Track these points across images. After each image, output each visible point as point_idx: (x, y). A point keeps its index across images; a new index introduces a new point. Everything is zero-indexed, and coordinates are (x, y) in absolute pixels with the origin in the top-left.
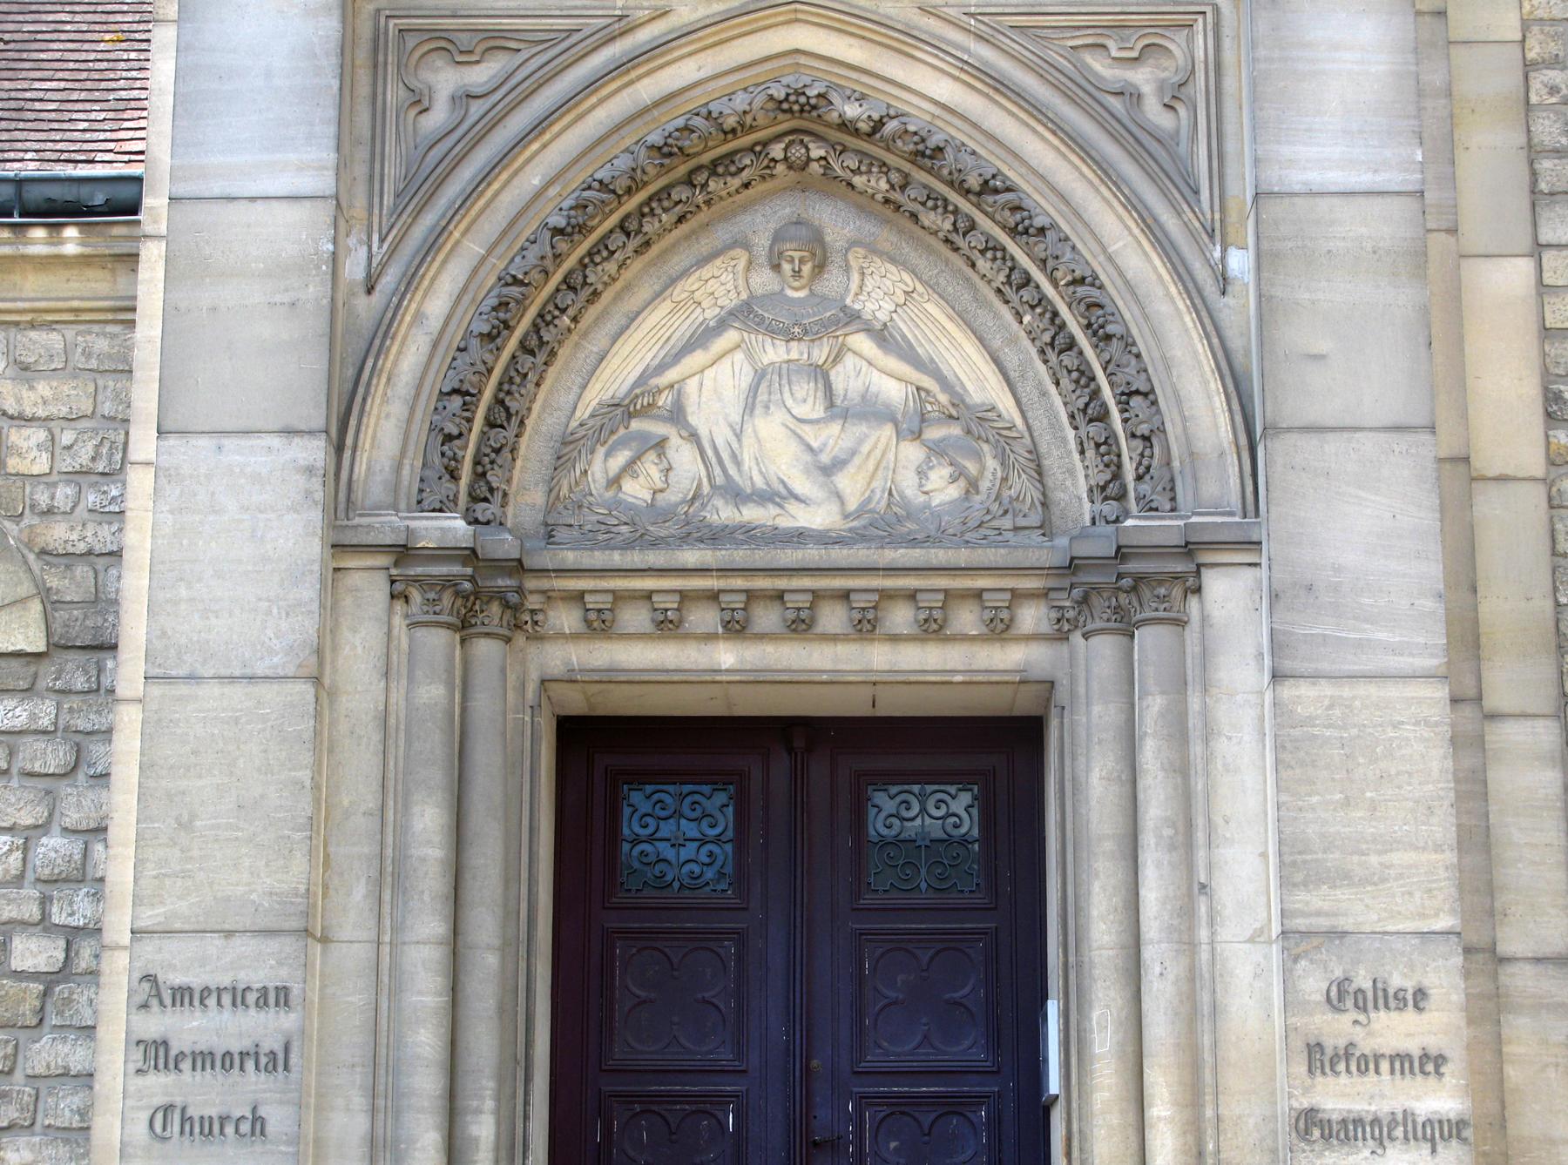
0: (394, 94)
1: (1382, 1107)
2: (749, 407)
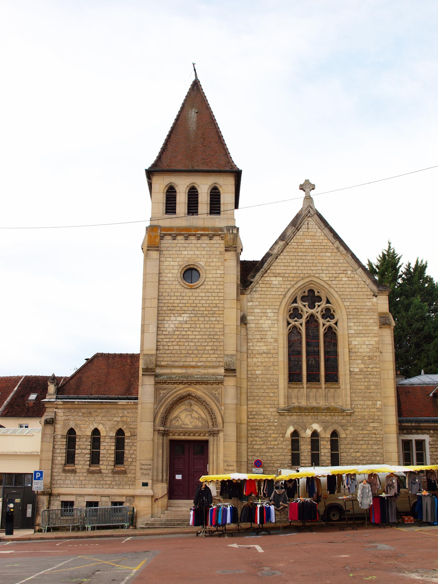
0: (158, 393)
2: (185, 417)
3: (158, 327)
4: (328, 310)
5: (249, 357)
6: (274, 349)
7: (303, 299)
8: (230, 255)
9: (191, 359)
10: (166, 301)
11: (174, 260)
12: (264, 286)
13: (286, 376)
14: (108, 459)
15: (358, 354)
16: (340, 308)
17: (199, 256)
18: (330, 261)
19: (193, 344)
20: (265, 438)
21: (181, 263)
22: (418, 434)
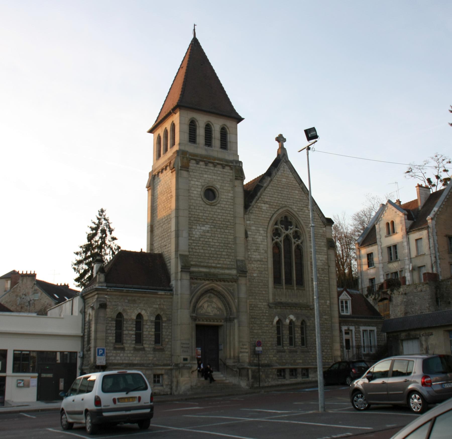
6: (265, 258)
8: (237, 183)
12: (257, 209)
14: (150, 339)
19: (213, 249)
21: (203, 184)
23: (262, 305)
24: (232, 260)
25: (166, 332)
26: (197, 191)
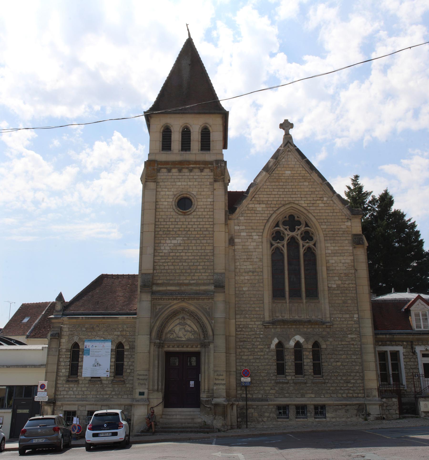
1: (220, 383)
2: (179, 331)
3: (155, 250)
4: (307, 232)
5: (236, 275)
6: (259, 268)
7: (284, 223)
8: (218, 185)
9: (184, 278)
10: (162, 226)
11: (170, 190)
13: (271, 292)
15: (335, 272)
16: (318, 231)
17: (191, 186)
18: (308, 190)
19: (186, 264)
20: (252, 349)
21: (175, 193)
22: (393, 345)
23: (255, 324)
24: (210, 274)
25: (128, 362)
26: (168, 202)
